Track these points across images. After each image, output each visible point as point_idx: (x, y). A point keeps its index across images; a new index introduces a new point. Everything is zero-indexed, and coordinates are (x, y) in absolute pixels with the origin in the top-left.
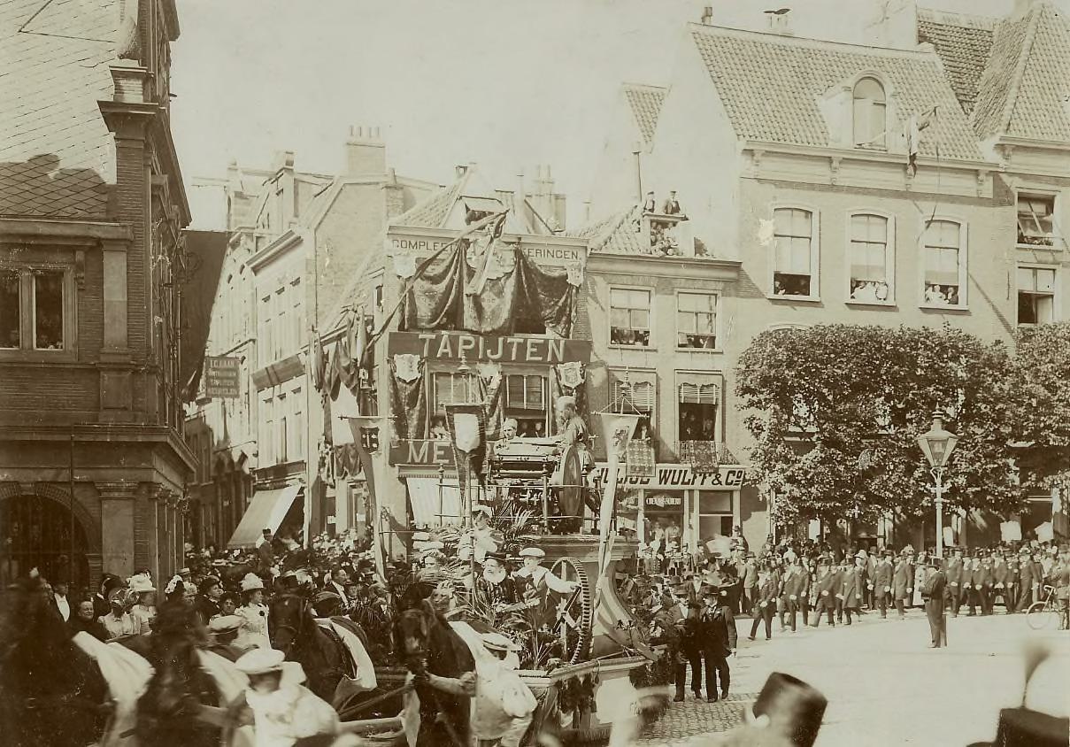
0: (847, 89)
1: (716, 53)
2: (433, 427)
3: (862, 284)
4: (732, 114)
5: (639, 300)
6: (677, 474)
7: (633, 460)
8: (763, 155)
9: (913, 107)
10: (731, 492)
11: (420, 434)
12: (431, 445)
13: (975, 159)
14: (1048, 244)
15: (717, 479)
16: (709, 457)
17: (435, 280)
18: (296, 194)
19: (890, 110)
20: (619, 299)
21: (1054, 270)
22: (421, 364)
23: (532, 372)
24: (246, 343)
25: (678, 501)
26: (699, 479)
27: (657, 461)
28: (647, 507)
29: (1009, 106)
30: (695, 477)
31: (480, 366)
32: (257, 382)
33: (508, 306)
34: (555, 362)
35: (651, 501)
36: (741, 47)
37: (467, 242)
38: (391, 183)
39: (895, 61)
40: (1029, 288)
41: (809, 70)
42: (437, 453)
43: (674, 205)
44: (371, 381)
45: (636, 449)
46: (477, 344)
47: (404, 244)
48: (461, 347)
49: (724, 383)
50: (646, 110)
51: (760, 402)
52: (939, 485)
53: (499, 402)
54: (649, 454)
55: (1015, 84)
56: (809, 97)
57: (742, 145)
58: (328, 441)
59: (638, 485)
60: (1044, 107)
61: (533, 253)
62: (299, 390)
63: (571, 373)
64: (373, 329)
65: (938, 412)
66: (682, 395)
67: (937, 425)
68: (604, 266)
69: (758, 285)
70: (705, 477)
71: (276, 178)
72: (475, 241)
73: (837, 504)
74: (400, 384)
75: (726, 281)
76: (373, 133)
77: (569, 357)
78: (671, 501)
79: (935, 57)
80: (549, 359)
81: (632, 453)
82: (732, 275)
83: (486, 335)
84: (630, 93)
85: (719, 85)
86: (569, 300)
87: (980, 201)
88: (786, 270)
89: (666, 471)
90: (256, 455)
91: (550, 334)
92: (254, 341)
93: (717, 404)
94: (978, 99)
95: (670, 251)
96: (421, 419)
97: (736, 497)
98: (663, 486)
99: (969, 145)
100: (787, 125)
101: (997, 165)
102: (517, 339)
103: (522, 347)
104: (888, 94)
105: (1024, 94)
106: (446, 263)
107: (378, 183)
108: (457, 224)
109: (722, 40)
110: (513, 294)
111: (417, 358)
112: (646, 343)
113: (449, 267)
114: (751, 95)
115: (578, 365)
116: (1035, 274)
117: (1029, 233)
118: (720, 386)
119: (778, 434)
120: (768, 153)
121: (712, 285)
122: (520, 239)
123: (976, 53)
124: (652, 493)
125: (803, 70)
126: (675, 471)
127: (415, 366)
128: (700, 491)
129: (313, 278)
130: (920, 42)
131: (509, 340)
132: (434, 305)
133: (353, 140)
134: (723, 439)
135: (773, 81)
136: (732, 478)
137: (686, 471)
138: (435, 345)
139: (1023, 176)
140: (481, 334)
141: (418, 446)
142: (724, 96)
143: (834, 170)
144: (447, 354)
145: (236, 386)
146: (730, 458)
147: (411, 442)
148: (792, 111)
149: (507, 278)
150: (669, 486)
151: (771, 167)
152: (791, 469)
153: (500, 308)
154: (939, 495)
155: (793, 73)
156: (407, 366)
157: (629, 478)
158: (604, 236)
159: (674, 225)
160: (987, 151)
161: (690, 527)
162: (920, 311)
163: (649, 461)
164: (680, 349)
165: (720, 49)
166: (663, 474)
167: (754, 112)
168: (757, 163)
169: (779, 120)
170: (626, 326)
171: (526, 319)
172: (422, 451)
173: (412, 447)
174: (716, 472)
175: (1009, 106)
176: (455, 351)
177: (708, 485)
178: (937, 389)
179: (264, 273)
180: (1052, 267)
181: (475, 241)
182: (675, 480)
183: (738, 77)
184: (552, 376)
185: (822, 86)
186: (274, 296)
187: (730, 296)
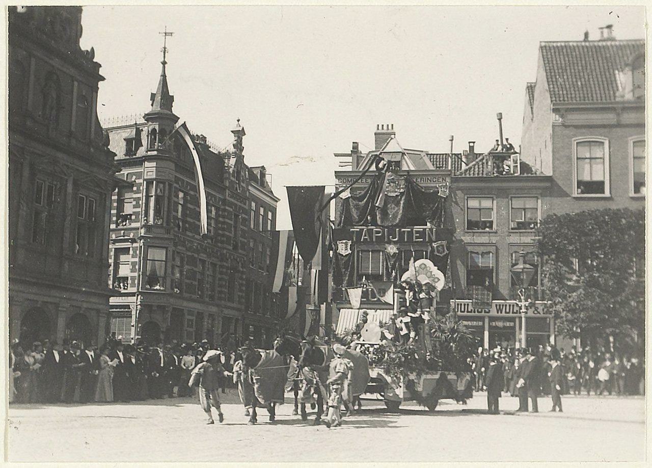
5: (486, 203)
6: (508, 307)
15: (536, 310)
17: (361, 199)
20: (473, 203)
25: (512, 324)
28: (490, 327)
33: (401, 212)
35: (494, 324)
43: (508, 146)
47: (345, 181)
48: (375, 235)
53: (397, 266)
54: (488, 295)
61: (419, 180)
66: (514, 258)
68: (461, 185)
73: (598, 324)
74: (339, 257)
75: (546, 188)
76: (390, 127)
78: (508, 324)
82: (548, 184)
86: (440, 206)
89: (500, 305)
96: (351, 276)
110: (403, 203)
113: (368, 191)
115: (444, 243)
120: (567, 110)
121: (534, 191)
124: (492, 319)
131: (402, 230)
133: (379, 131)
144: (367, 239)
150: (504, 314)
153: (397, 212)
157: (476, 310)
164: (513, 231)
166: (498, 307)
168: (562, 116)
170: (474, 218)
171: (413, 217)
176: (371, 237)
187: (546, 197)
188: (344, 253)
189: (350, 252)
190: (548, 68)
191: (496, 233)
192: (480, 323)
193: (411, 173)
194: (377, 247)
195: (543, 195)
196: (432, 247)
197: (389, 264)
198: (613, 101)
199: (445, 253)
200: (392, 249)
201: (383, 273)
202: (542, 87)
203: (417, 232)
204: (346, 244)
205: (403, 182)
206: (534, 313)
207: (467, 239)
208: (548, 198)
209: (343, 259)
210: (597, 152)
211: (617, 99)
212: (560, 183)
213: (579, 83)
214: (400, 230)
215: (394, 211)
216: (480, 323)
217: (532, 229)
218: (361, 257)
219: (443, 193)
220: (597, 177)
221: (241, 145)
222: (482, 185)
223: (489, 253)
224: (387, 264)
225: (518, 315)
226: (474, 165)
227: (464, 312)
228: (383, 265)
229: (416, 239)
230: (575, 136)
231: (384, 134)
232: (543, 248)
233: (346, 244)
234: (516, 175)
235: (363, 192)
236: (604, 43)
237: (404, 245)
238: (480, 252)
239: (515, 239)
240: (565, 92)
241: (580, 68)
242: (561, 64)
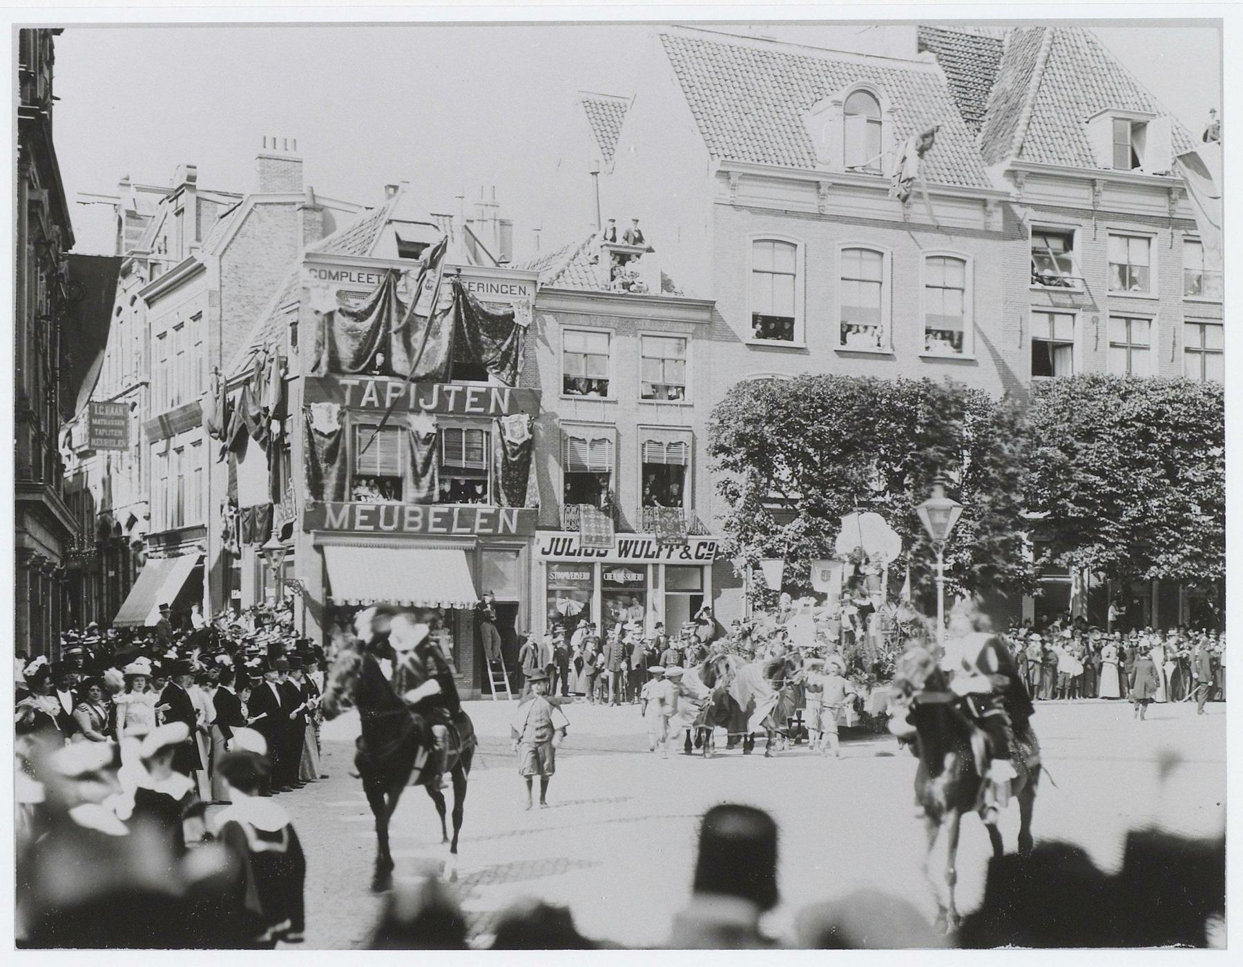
0: (837, 103)
1: (687, 59)
2: (355, 487)
4: (705, 130)
5: (596, 344)
7: (589, 529)
8: (740, 178)
9: (912, 125)
10: (701, 567)
11: (339, 496)
12: (352, 510)
13: (983, 187)
14: (1067, 285)
15: (686, 551)
16: (677, 526)
17: (360, 317)
18: (198, 215)
19: (887, 128)
20: (575, 342)
21: (1073, 315)
22: (341, 415)
24: (137, 386)
25: (640, 577)
26: (665, 552)
27: (617, 531)
28: (605, 583)
29: (1022, 126)
30: (660, 549)
31: (412, 418)
32: (149, 432)
34: (499, 413)
35: (609, 577)
36: (716, 51)
37: (397, 274)
38: (308, 203)
39: (892, 72)
40: (1044, 335)
41: (793, 81)
42: (359, 518)
44: (283, 434)
45: (592, 516)
46: (408, 393)
49: (694, 439)
50: (606, 122)
51: (735, 463)
52: (940, 561)
55: (1029, 102)
56: (794, 111)
57: (717, 165)
58: (233, 503)
59: (594, 558)
60: (1061, 129)
61: (474, 287)
62: (197, 443)
63: (516, 428)
64: (286, 373)
65: (939, 477)
66: (646, 454)
67: (938, 492)
69: (733, 328)
70: (671, 550)
71: (175, 195)
72: (406, 273)
74: (317, 437)
75: (699, 323)
77: (514, 409)
78: (632, 577)
79: (937, 69)
80: (492, 410)
81: (588, 520)
82: (704, 316)
83: (416, 380)
84: (587, 103)
85: (690, 96)
86: (515, 343)
87: (988, 234)
88: (766, 311)
90: (148, 518)
91: (493, 381)
92: (146, 384)
93: (686, 466)
94: (986, 118)
95: (632, 288)
96: (341, 478)
97: (708, 572)
98: (623, 560)
99: (975, 170)
100: (768, 143)
101: (1008, 195)
102: (455, 386)
103: (461, 396)
104: (884, 112)
105: (1038, 113)
106: (373, 297)
107: (294, 204)
108: (387, 252)
109: (694, 43)
110: (450, 334)
111: (336, 408)
112: (604, 393)
113: (376, 302)
114: (727, 108)
115: (525, 418)
116: (1052, 320)
117: (1047, 273)
118: (689, 443)
119: (757, 499)
120: (745, 176)
122: (459, 270)
123: (984, 65)
125: (786, 80)
126: (637, 542)
127: (335, 416)
128: (667, 566)
129: (216, 311)
130: (920, 51)
131: (446, 388)
132: (356, 346)
134: (693, 507)
135: (752, 93)
136: (703, 550)
137: (650, 543)
138: (359, 391)
139: (1037, 207)
140: (413, 380)
142: (696, 109)
143: (823, 197)
144: (373, 402)
145: (125, 437)
146: (700, 527)
147: (328, 506)
148: (774, 127)
149: (444, 316)
150: (630, 559)
152: (771, 541)
153: (438, 350)
154: (940, 573)
155: (775, 84)
157: (583, 550)
158: (557, 269)
159: (638, 256)
160: (996, 178)
161: (654, 609)
162: (920, 361)
163: (607, 530)
165: (691, 53)
167: (729, 127)
169: (759, 138)
170: (580, 372)
172: (341, 516)
173: (330, 512)
174: (685, 542)
175: (1022, 126)
176: (381, 400)
177: (675, 559)
178: (938, 450)
179: (161, 306)
180: (1072, 311)
181: (406, 273)
182: (638, 553)
183: (712, 87)
184: (495, 430)
185: (809, 101)
186: (171, 332)
190: (684, 82)
191: (616, 402)
194: (392, 420)
195: (694, 335)
198: (811, 168)
200: (423, 424)
203: (474, 394)
206: (681, 557)
208: (706, 343)
209: (324, 442)
211: (819, 168)
214: (440, 389)
217: (671, 398)
218: (360, 439)
219: (522, 318)
225: (654, 560)
228: (404, 458)
229: (472, 407)
237: (446, 418)
238: (589, 440)
239: (650, 414)
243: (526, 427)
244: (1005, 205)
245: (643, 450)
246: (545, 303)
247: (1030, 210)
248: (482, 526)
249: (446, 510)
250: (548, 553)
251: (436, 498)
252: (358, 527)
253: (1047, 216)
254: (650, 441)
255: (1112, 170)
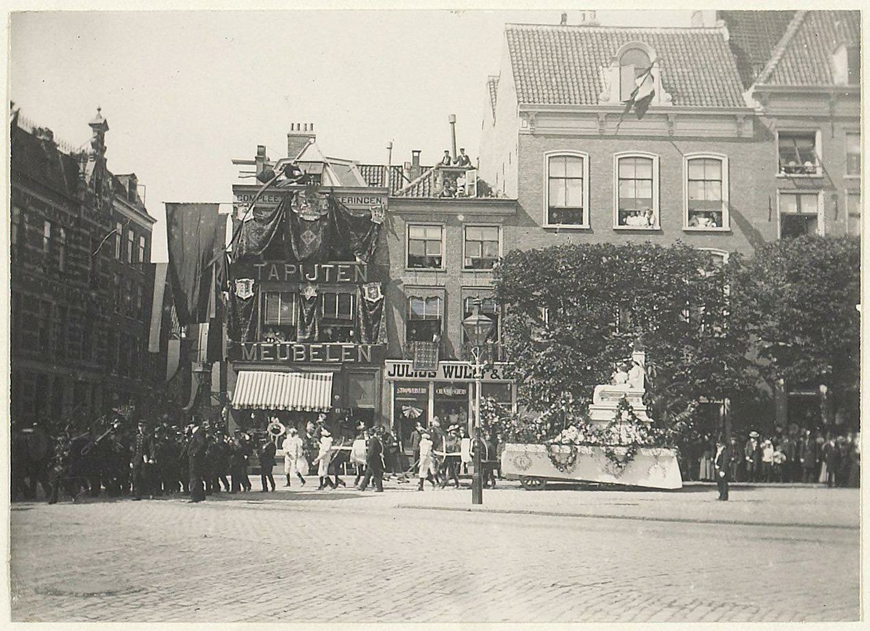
3: (632, 214)
5: (433, 233)
7: (419, 359)
20: (416, 233)
23: (343, 291)
25: (464, 392)
35: (441, 391)
37: (292, 195)
43: (464, 159)
54: (435, 353)
61: (346, 200)
66: (467, 306)
68: (401, 208)
72: (297, 194)
74: (238, 301)
76: (309, 127)
78: (458, 392)
81: (420, 352)
87: (739, 139)
89: (448, 367)
101: (752, 110)
103: (333, 272)
126: (457, 367)
131: (323, 266)
133: (293, 133)
138: (266, 271)
139: (779, 117)
141: (249, 347)
151: (545, 125)
156: (244, 290)
173: (244, 350)
188: (244, 295)
189: (253, 294)
191: (446, 272)
192: (424, 391)
193: (335, 191)
196: (363, 291)
197: (304, 312)
199: (378, 299)
201: (296, 323)
202: (507, 84)
204: (247, 283)
205: (325, 202)
207: (408, 279)
208: (513, 228)
210: (574, 170)
212: (527, 209)
213: (554, 80)
215: (311, 240)
216: (424, 391)
220: (574, 203)
221: (102, 143)
222: (428, 208)
223: (436, 297)
224: (302, 312)
225: (472, 379)
226: (420, 183)
227: (402, 375)
230: (546, 148)
231: (300, 136)
232: (503, 293)
233: (247, 283)
234: (471, 197)
235: (269, 214)
236: (586, 30)
239: (469, 280)
240: (535, 91)
241: (555, 60)
242: (532, 54)
243: (379, 290)
244: (755, 118)
245: (465, 304)
246: (392, 209)
247: (775, 120)
248: (346, 357)
249: (320, 346)
250: (394, 375)
251: (316, 339)
252: (312, 359)
253: (790, 123)
254: (469, 298)
255: (847, 86)
